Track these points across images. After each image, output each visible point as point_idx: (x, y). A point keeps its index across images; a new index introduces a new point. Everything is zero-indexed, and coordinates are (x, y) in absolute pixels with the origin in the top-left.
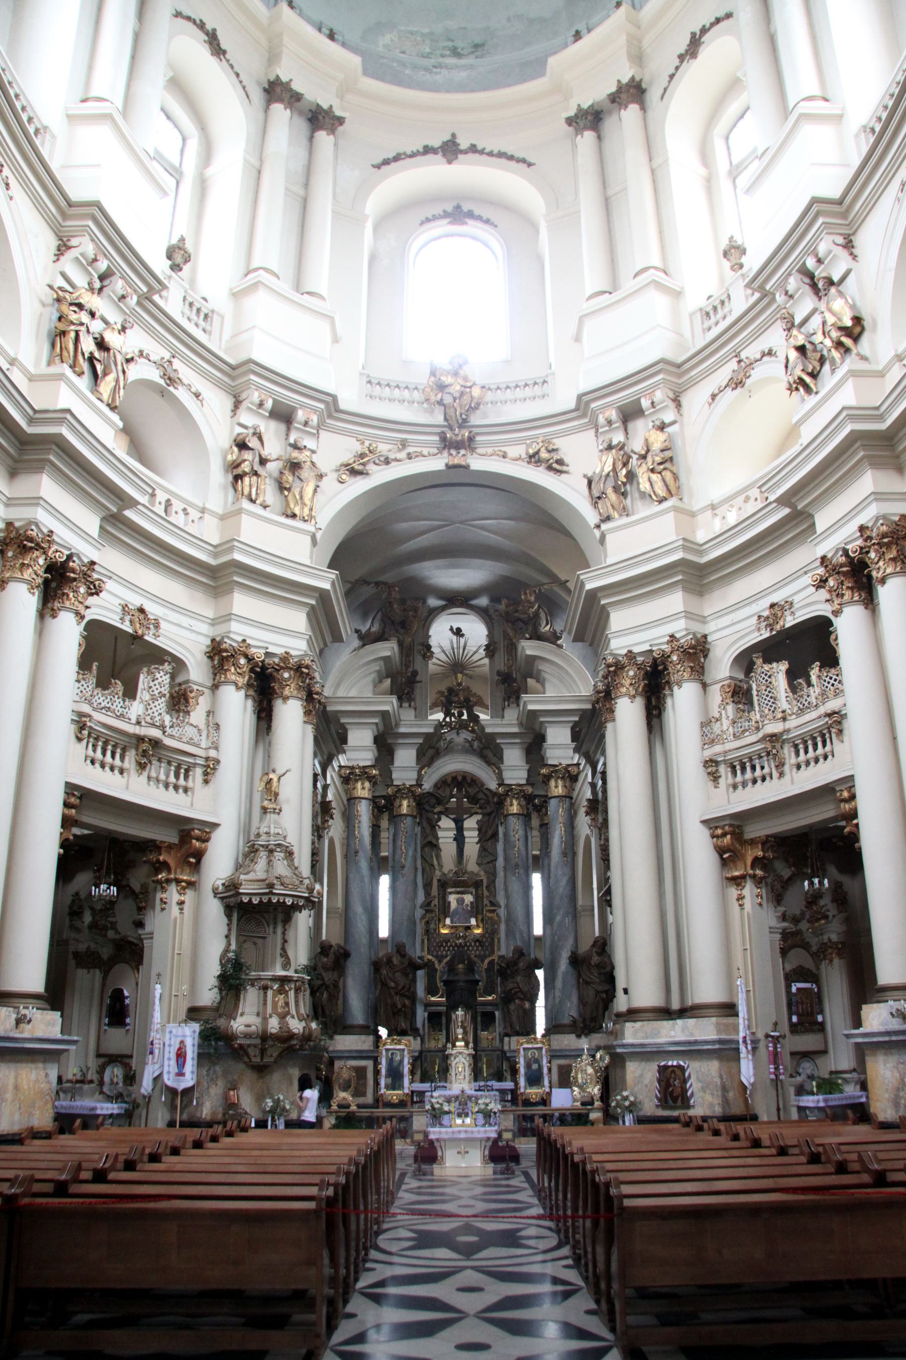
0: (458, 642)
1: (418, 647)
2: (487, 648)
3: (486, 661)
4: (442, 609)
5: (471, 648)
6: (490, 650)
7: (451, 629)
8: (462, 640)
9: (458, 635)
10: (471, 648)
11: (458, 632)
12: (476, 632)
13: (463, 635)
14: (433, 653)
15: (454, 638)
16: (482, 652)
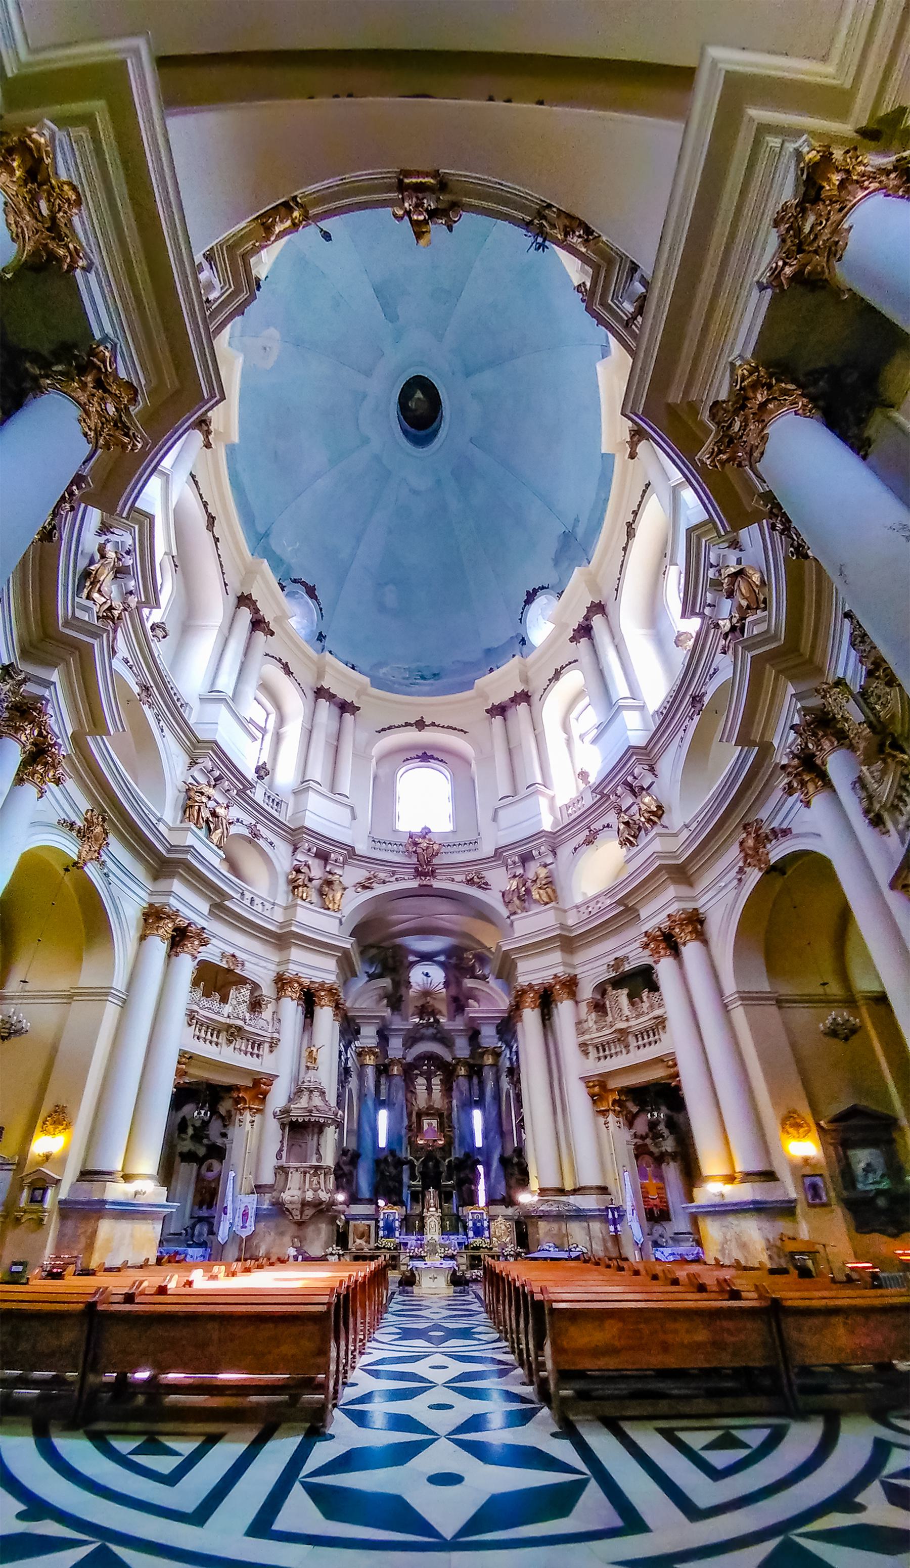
3: (444, 990)
4: (418, 962)
5: (435, 983)
6: (447, 984)
9: (427, 977)
10: (435, 983)
11: (427, 975)
12: (437, 975)
16: (441, 986)
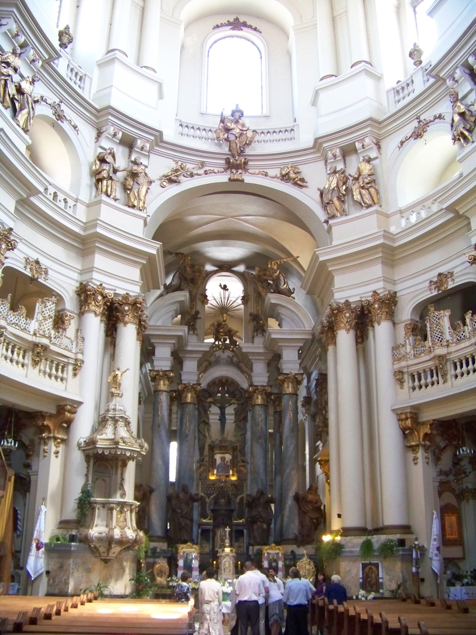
0: (225, 294)
1: (198, 296)
2: (243, 298)
3: (242, 307)
4: (215, 272)
5: (232, 299)
6: (245, 299)
7: (220, 286)
8: (227, 293)
9: (224, 290)
10: (232, 299)
11: (225, 288)
12: (236, 289)
13: (227, 290)
14: (208, 300)
15: (222, 290)
16: (239, 301)
